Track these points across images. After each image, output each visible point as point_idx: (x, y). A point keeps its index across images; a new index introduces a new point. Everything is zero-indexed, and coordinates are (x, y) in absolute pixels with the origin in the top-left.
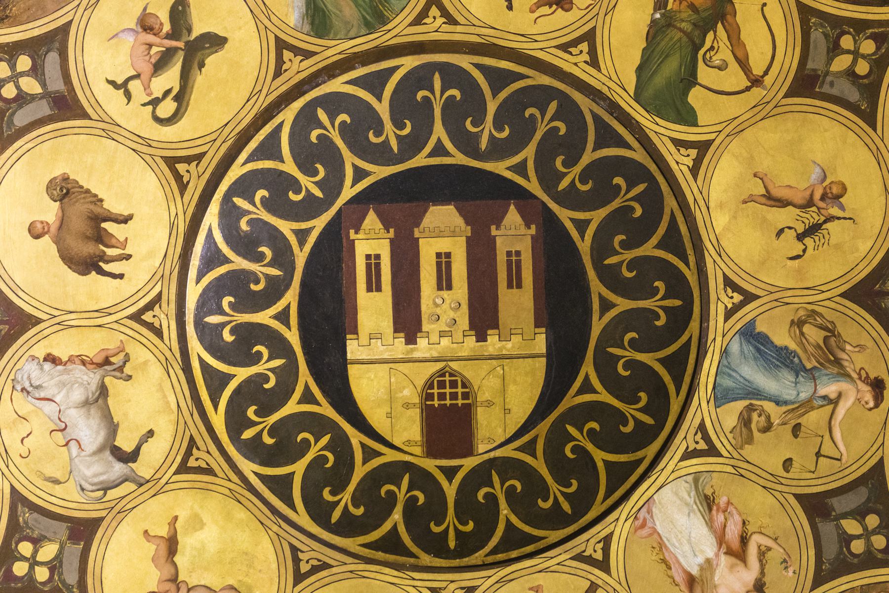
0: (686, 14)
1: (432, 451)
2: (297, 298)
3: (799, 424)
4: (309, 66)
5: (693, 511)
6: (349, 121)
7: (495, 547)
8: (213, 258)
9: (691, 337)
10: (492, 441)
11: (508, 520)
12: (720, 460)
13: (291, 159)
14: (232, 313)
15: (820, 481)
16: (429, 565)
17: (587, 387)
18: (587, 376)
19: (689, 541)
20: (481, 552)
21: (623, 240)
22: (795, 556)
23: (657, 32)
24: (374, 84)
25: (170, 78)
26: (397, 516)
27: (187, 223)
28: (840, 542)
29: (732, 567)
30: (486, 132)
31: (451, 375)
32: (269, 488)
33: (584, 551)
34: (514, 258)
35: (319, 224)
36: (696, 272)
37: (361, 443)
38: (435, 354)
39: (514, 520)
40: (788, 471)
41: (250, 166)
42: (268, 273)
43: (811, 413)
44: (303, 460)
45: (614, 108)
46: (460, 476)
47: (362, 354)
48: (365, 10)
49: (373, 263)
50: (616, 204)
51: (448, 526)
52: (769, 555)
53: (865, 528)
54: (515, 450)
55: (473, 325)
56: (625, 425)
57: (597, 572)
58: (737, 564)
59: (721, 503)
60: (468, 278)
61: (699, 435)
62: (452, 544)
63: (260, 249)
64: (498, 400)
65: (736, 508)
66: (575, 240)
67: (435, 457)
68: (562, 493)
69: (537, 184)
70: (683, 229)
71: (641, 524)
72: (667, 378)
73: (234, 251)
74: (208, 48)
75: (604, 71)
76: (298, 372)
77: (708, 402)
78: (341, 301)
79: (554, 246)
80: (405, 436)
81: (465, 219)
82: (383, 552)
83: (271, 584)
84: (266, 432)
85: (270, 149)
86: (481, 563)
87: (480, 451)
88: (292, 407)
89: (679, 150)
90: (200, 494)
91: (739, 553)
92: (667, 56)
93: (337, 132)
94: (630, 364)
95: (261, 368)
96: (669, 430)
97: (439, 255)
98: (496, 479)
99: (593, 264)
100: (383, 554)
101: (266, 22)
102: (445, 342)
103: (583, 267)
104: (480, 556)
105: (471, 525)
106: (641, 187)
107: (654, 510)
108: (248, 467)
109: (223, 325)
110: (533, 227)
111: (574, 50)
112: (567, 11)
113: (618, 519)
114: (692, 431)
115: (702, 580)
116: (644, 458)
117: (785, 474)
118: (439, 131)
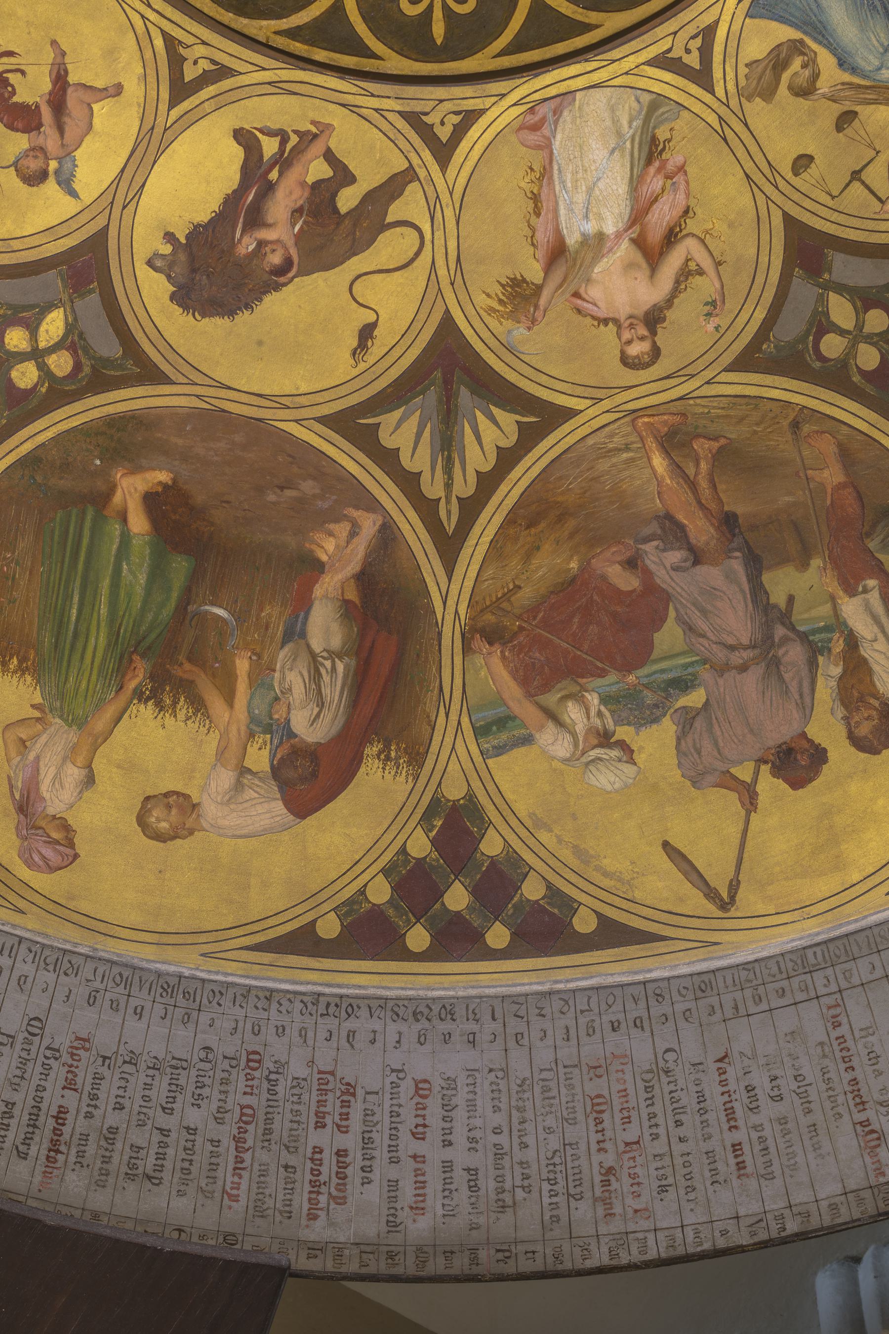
3: (856, 113)
7: (298, 27)
15: (835, 217)
19: (590, 191)
20: (273, 22)
22: (732, 305)
28: (811, 324)
29: (630, 266)
33: (426, 114)
40: (796, 174)
43: (882, 107)
52: (697, 280)
53: (859, 326)
57: (427, 155)
58: (639, 267)
59: (671, 162)
61: (698, 42)
65: (687, 182)
71: (536, 125)
91: (652, 253)
107: (566, 113)
113: (504, 95)
114: (691, 30)
115: (575, 260)
116: (597, 27)
117: (789, 176)
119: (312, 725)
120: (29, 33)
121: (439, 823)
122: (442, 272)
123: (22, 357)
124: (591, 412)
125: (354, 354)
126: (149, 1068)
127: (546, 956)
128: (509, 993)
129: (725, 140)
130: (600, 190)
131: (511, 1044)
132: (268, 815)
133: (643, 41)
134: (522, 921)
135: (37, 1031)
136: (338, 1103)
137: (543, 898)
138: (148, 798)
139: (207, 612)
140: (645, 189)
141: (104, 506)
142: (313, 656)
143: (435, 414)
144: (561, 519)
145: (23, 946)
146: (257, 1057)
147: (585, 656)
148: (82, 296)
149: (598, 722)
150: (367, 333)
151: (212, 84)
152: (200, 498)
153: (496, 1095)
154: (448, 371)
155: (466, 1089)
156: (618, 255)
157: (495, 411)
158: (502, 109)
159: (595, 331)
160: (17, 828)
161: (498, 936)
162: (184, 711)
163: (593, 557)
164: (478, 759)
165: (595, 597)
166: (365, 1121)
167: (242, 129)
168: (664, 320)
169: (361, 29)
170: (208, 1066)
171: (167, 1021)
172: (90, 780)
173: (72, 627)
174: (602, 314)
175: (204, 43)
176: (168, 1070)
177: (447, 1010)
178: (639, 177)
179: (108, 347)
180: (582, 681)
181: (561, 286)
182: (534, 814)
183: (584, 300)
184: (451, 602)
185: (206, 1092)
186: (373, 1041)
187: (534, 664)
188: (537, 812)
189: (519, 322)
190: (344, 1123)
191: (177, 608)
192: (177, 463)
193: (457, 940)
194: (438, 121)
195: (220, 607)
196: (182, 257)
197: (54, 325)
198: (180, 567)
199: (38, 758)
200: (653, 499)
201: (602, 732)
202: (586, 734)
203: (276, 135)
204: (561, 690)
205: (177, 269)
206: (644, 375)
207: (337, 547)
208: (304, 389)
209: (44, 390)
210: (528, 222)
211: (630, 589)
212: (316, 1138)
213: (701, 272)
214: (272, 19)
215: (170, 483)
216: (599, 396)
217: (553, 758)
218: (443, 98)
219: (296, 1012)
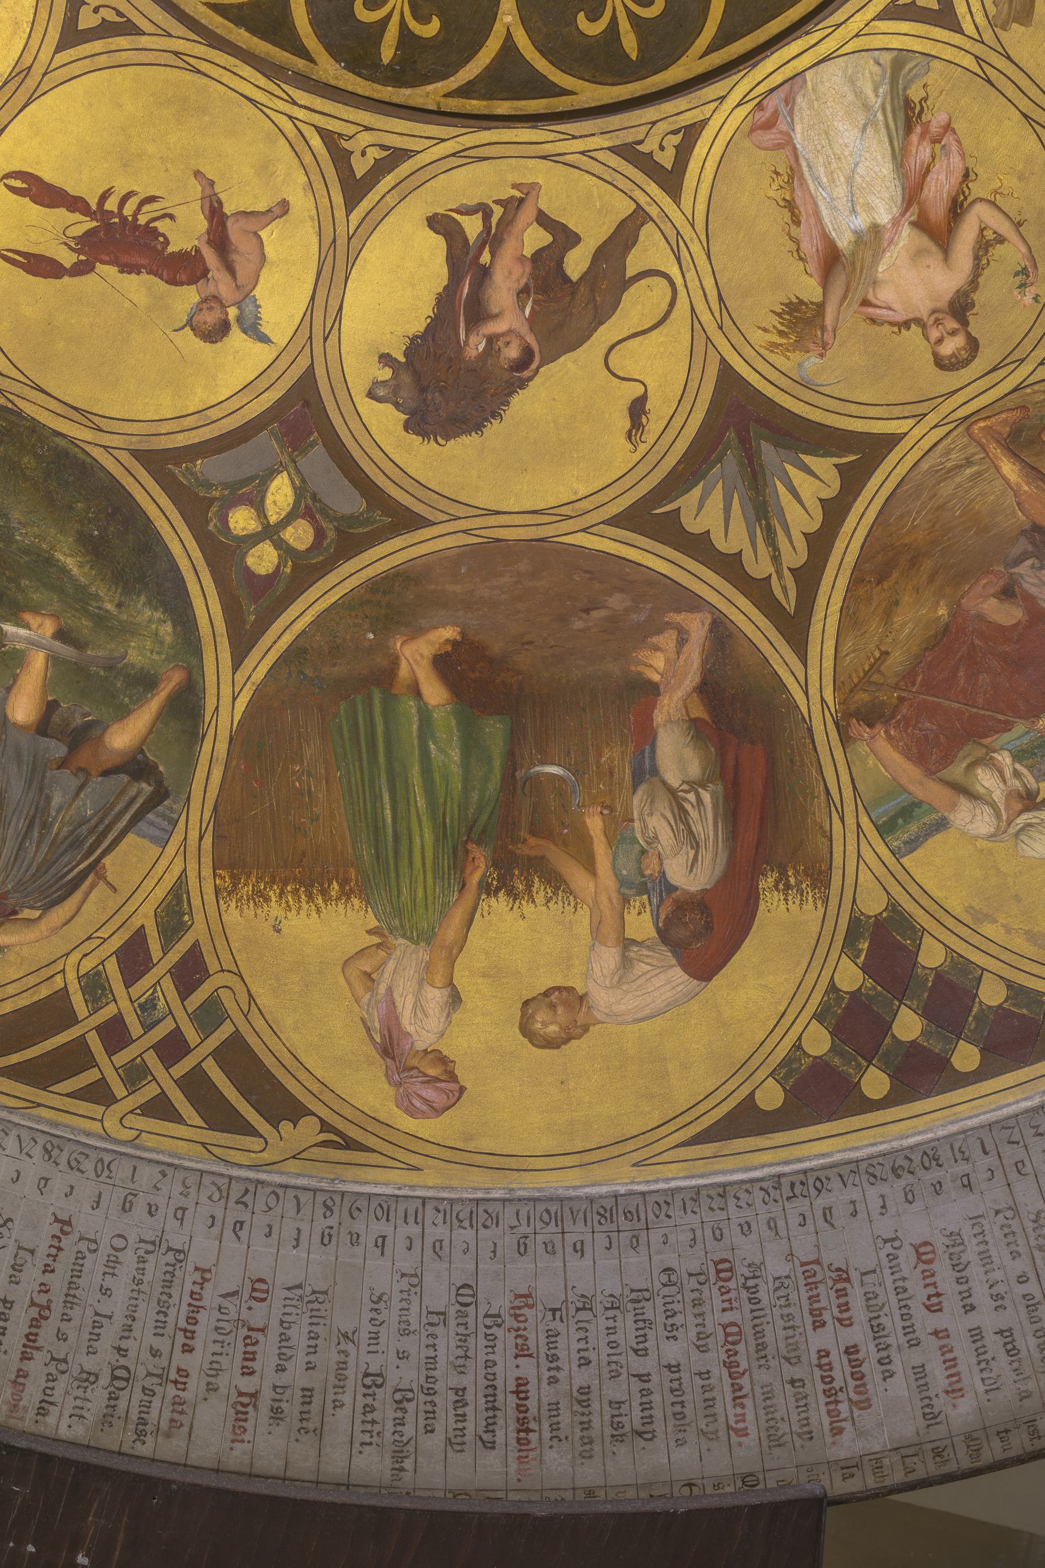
5: (875, 124)
12: (956, 38)
16: (333, 82)
19: (850, 180)
20: (439, 85)
29: (918, 254)
33: (641, 142)
39: (522, 40)
51: (389, 16)
52: (999, 250)
57: (654, 189)
58: (928, 252)
59: (934, 123)
62: (387, 53)
65: (958, 141)
68: (630, 14)
71: (768, 121)
82: (248, 30)
83: (14, 33)
86: (433, 107)
91: (939, 232)
100: (247, 34)
105: (435, 24)
107: (799, 99)
113: (723, 98)
115: (853, 263)
119: (691, 872)
120: (167, 170)
121: (865, 945)
122: (705, 317)
123: (253, 540)
124: (917, 432)
125: (629, 437)
126: (607, 1309)
127: (1026, 1065)
128: (995, 1119)
129: (989, 81)
130: (861, 176)
131: (1013, 1176)
132: (668, 987)
134: (989, 1033)
135: (469, 1300)
136: (833, 1294)
137: (1006, 1001)
138: (526, 1003)
139: (538, 774)
140: (912, 161)
141: (391, 685)
142: (672, 792)
144: (914, 563)
145: (429, 1208)
146: (727, 1265)
147: (982, 712)
148: (304, 452)
149: (1016, 783)
150: (637, 409)
151: (389, 173)
152: (497, 648)
153: (1011, 1238)
154: (743, 428)
155: (975, 1241)
156: (901, 244)
157: (807, 459)
158: (725, 113)
159: (897, 339)
160: (387, 1075)
161: (966, 1056)
162: (542, 893)
163: (962, 597)
164: (890, 860)
165: (977, 642)
166: (868, 1307)
167: (436, 215)
168: (973, 305)
169: (542, 65)
170: (674, 1290)
171: (614, 1251)
172: (455, 999)
173: (390, 830)
174: (899, 318)
175: (367, 129)
176: (630, 1306)
177: (930, 1156)
178: (901, 149)
179: (348, 502)
180: (985, 741)
181: (844, 298)
182: (972, 907)
183: (875, 306)
184: (813, 690)
185: (678, 1320)
186: (854, 1214)
187: (926, 736)
188: (974, 904)
189: (808, 351)
190: (845, 1315)
191: (503, 778)
192: (460, 613)
193: (920, 1074)
194: (656, 147)
195: (552, 764)
196: (406, 378)
197: (280, 494)
198: (495, 730)
199: (390, 990)
200: (1014, 512)
201: (1024, 794)
202: (1007, 800)
203: (476, 212)
204: (965, 757)
205: (404, 393)
206: (965, 374)
207: (667, 661)
208: (583, 491)
209: (288, 570)
210: (789, 234)
211: (1014, 622)
212: (817, 1340)
213: (1001, 240)
214: (438, 81)
215: (458, 638)
216: (920, 412)
217: (976, 837)
218: (655, 119)
219: (758, 1201)
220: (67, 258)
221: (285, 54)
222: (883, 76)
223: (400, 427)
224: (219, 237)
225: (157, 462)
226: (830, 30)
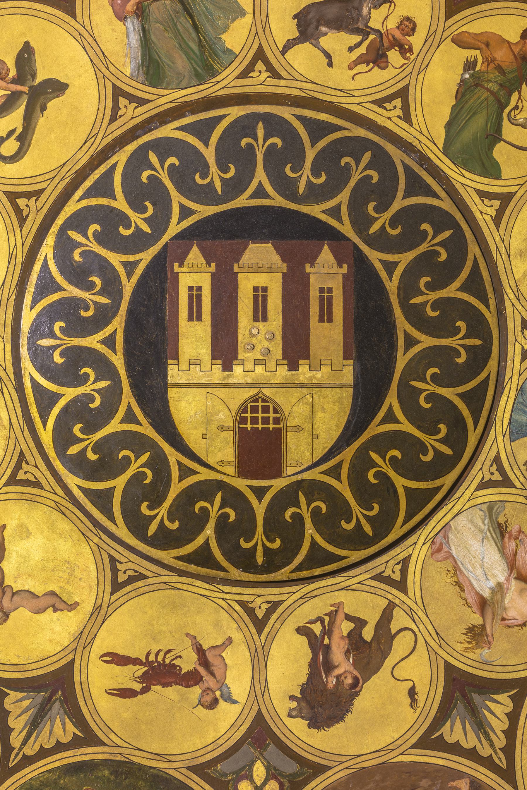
0: (494, 75)
1: (243, 472)
2: (123, 324)
4: (142, 113)
6: (177, 163)
7: (300, 564)
8: (47, 286)
9: (489, 374)
10: (300, 464)
11: (313, 539)
12: (514, 491)
13: (123, 197)
14: (62, 337)
16: (238, 579)
17: (390, 417)
18: (390, 407)
19: (482, 566)
20: (287, 568)
21: (428, 281)
23: (466, 91)
24: (203, 131)
25: (15, 119)
26: (209, 531)
27: (25, 254)
30: (305, 177)
31: (264, 401)
32: (91, 501)
33: (383, 572)
34: (326, 294)
35: (146, 257)
36: (496, 314)
37: (178, 461)
38: (249, 381)
39: (319, 539)
41: (85, 203)
42: (97, 300)
44: (123, 476)
45: (423, 160)
46: (268, 497)
47: (183, 379)
48: (195, 62)
49: (195, 294)
50: (423, 248)
51: (257, 543)
54: (321, 473)
55: (285, 356)
56: (425, 454)
57: (394, 591)
59: (513, 531)
60: (283, 311)
61: (495, 466)
62: (260, 560)
63: (91, 279)
64: (307, 426)
66: (384, 280)
67: (247, 478)
68: (365, 516)
69: (350, 227)
70: (485, 274)
71: (439, 548)
72: (466, 412)
73: (67, 280)
74: (50, 93)
75: (416, 126)
76: (121, 393)
77: (504, 436)
78: (164, 329)
79: (364, 286)
80: (219, 456)
81: (281, 256)
82: (195, 565)
84: (90, 448)
85: (104, 187)
86: (286, 579)
87: (289, 473)
88: (115, 426)
89: (483, 201)
90: (26, 505)
92: (474, 114)
93: (166, 173)
94: (432, 397)
95: (87, 388)
96: (467, 461)
97: (256, 289)
98: (302, 499)
99: (399, 303)
100: (195, 567)
101: (104, 70)
102: (259, 370)
103: (390, 306)
104: (285, 572)
105: (278, 542)
106: (447, 234)
107: (450, 535)
108: (73, 481)
109: (54, 348)
110: (345, 266)
111: (387, 105)
112: (383, 69)
113: (416, 543)
114: (488, 463)
115: (493, 603)
116: (442, 486)
118: (260, 175)
122: (432, 643)
125: (412, 706)
130: (487, 563)
133: (468, 481)
143: (467, 714)
148: (265, 749)
150: (412, 693)
151: (274, 613)
154: (462, 690)
156: (513, 589)
157: (495, 697)
158: (418, 549)
159: (522, 632)
169: (330, 548)
174: (521, 622)
175: (259, 596)
178: (502, 546)
179: (292, 767)
181: (493, 619)
183: (508, 620)
189: (483, 648)
194: (391, 572)
196: (304, 704)
203: (317, 621)
205: (304, 711)
210: (461, 597)
220: (138, 687)
221: (214, 571)
222: (485, 515)
223: (307, 727)
224: (204, 661)
225: (199, 770)
226: (456, 501)
